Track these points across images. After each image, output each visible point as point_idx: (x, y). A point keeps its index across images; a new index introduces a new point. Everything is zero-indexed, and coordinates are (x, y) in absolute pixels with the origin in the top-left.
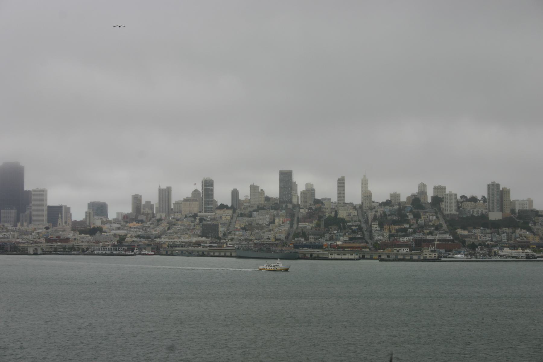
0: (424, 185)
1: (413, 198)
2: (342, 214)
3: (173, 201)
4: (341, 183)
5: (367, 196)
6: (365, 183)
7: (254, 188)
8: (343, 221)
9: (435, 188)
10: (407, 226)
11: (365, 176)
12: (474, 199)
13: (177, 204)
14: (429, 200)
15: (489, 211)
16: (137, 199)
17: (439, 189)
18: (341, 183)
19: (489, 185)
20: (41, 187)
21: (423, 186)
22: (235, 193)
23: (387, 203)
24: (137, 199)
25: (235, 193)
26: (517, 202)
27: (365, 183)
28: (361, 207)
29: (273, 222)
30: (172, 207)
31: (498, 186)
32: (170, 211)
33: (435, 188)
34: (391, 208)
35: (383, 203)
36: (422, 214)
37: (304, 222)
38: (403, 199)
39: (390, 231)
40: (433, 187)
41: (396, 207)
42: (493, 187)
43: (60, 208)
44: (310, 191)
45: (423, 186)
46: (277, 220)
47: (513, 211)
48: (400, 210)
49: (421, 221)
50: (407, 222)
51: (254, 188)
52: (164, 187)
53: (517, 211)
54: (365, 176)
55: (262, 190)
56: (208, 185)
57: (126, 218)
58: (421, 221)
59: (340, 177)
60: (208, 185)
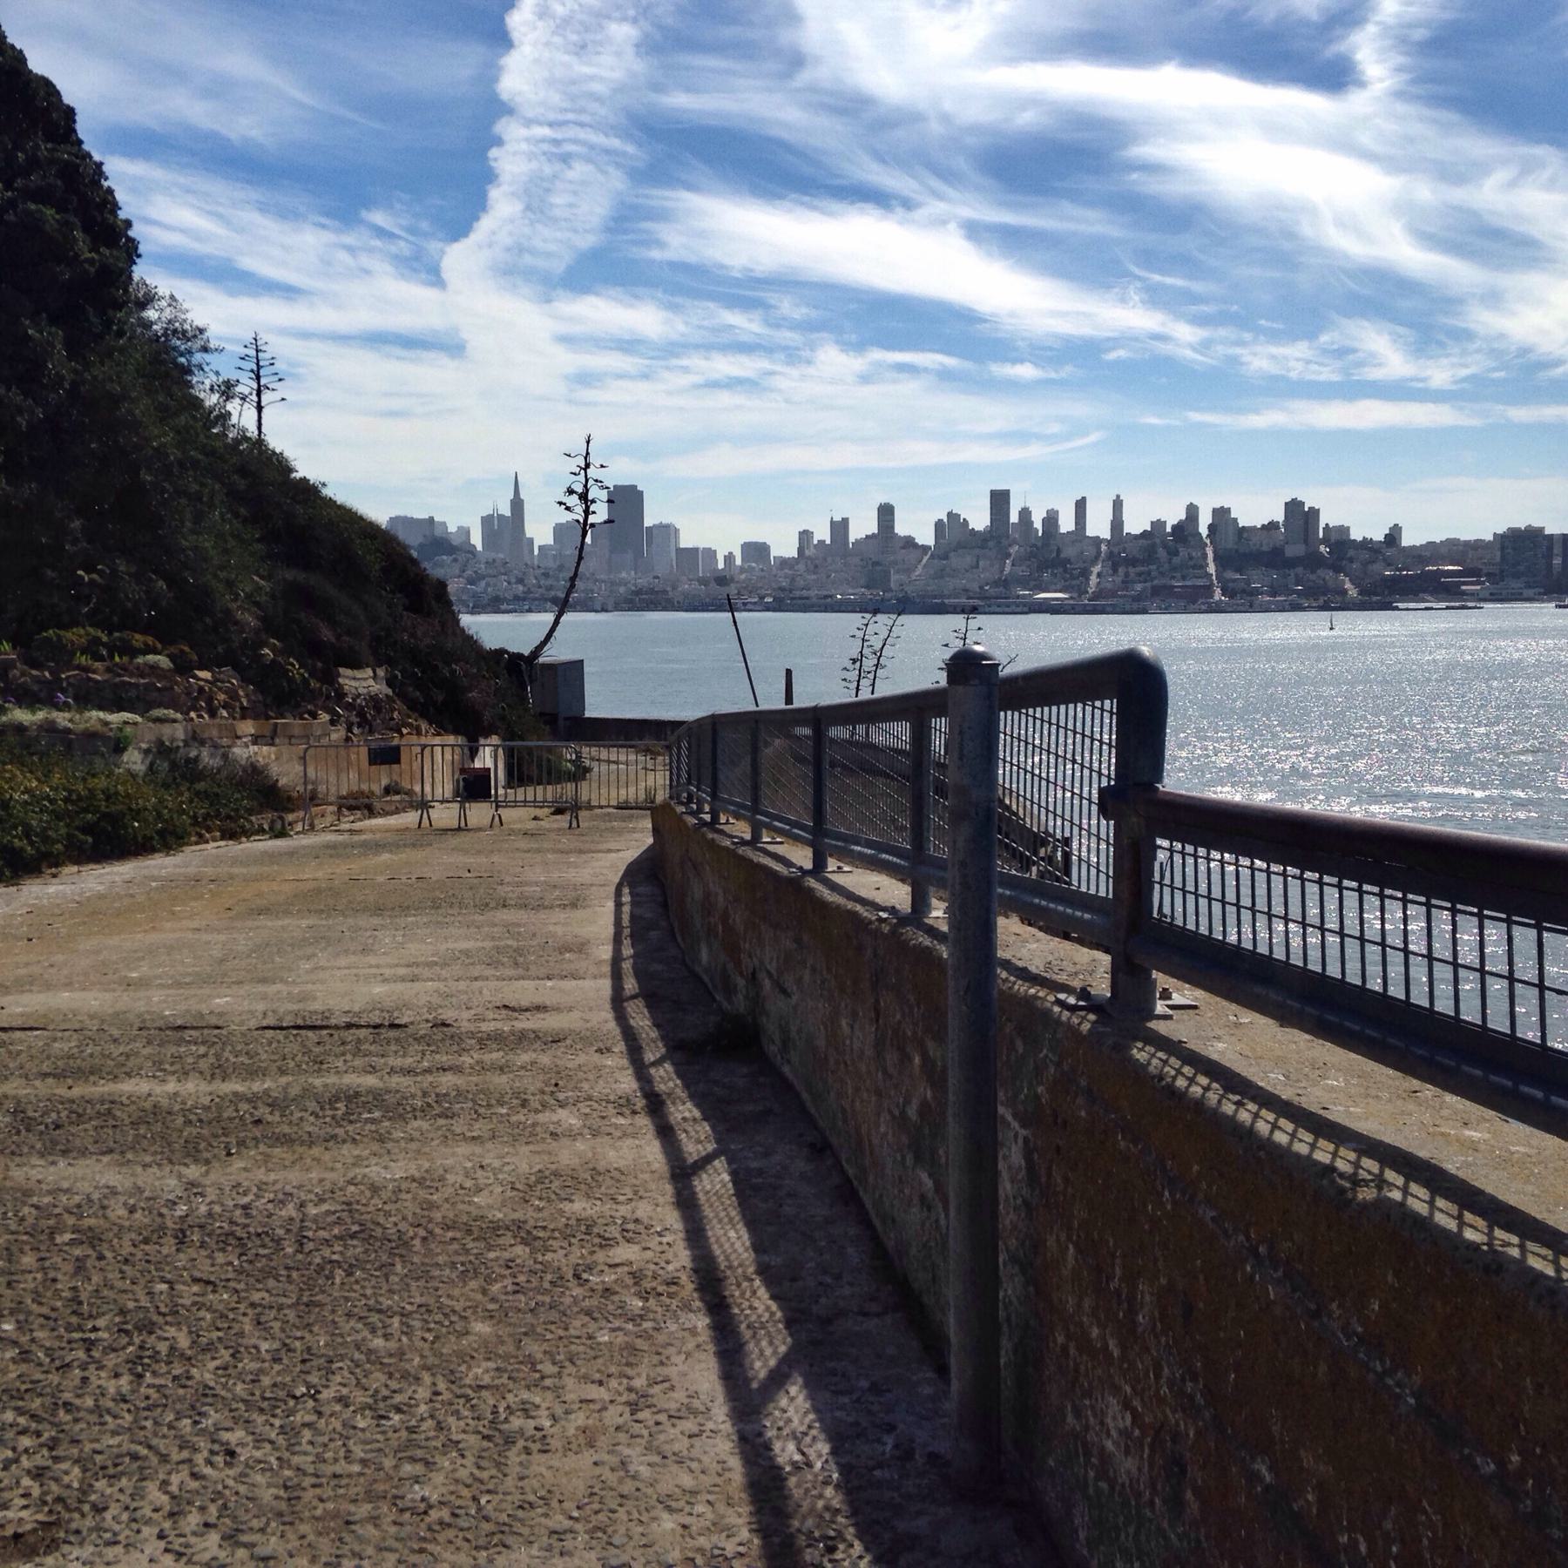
3: (852, 539)
4: (1081, 506)
6: (1118, 505)
9: (1215, 511)
11: (1118, 496)
13: (857, 542)
16: (805, 536)
18: (1081, 506)
21: (1192, 511)
23: (1145, 534)
24: (805, 536)
27: (1118, 505)
31: (1303, 504)
33: (1215, 511)
43: (694, 551)
45: (1192, 511)
52: (837, 518)
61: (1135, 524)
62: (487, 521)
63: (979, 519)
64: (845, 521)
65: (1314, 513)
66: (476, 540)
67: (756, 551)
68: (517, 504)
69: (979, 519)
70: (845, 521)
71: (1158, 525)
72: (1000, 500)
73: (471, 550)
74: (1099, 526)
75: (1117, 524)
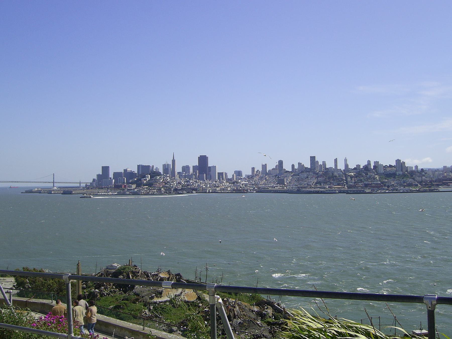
0: (370, 161)
1: (365, 166)
2: (336, 174)
3: (268, 170)
4: (336, 161)
5: (346, 166)
6: (346, 160)
7: (300, 164)
8: (336, 176)
10: (362, 178)
11: (346, 158)
12: (390, 166)
13: (269, 171)
14: (372, 168)
15: (397, 171)
17: (376, 163)
18: (336, 161)
19: (396, 160)
20: (215, 165)
21: (369, 162)
22: (293, 166)
23: (355, 169)
25: (293, 166)
26: (408, 167)
27: (346, 160)
28: (344, 170)
29: (308, 178)
30: (268, 172)
32: (267, 174)
34: (356, 171)
35: (353, 169)
36: (369, 173)
37: (320, 177)
38: (361, 167)
39: (355, 181)
40: (374, 162)
41: (358, 170)
42: (398, 161)
44: (324, 163)
45: (369, 162)
46: (309, 177)
47: (407, 171)
48: (359, 172)
49: (368, 176)
50: (363, 176)
51: (300, 164)
53: (409, 171)
54: (346, 158)
55: (303, 164)
56: (281, 163)
57: (248, 177)
58: (368, 176)
59: (335, 158)
60: (281, 163)
61: (352, 166)
62: (164, 166)
63: (308, 165)
64: (266, 164)
65: (404, 163)
66: (161, 171)
67: (239, 173)
68: (174, 161)
69: (308, 165)
70: (266, 164)
71: (358, 166)
72: (313, 159)
73: (159, 174)
74: (341, 166)
75: (346, 166)
